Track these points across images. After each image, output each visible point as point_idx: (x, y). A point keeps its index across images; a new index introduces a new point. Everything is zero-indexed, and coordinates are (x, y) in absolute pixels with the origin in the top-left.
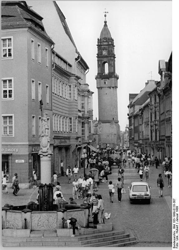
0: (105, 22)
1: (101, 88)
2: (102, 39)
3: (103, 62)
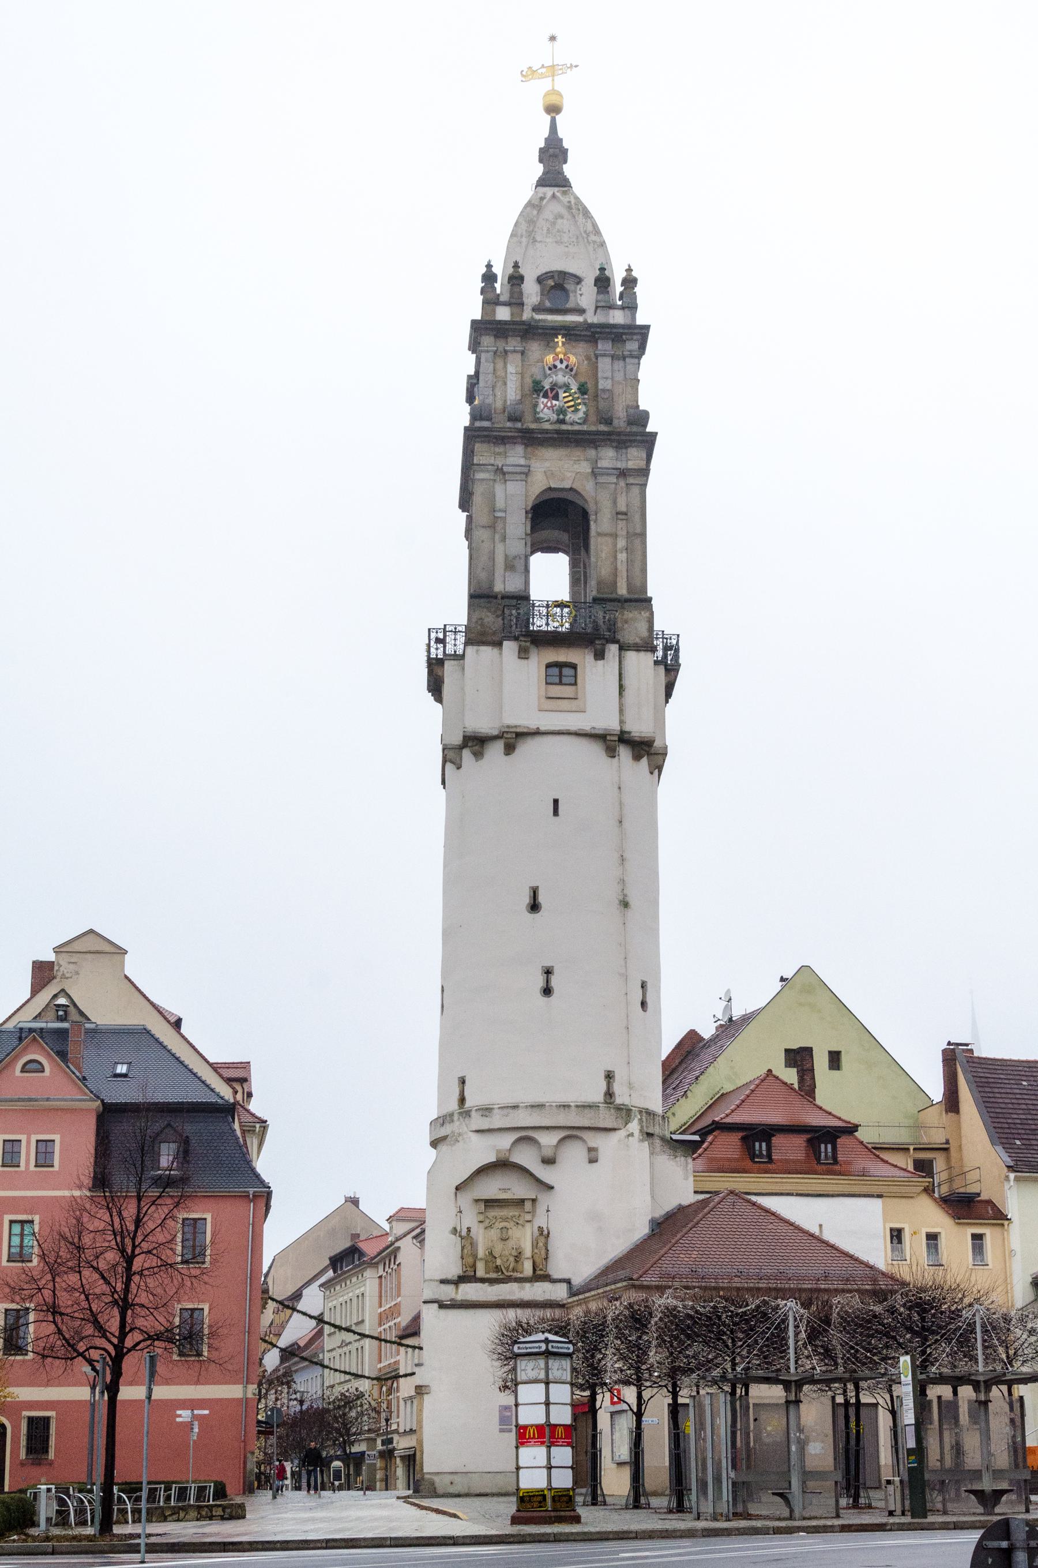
1: (512, 739)
2: (530, 275)
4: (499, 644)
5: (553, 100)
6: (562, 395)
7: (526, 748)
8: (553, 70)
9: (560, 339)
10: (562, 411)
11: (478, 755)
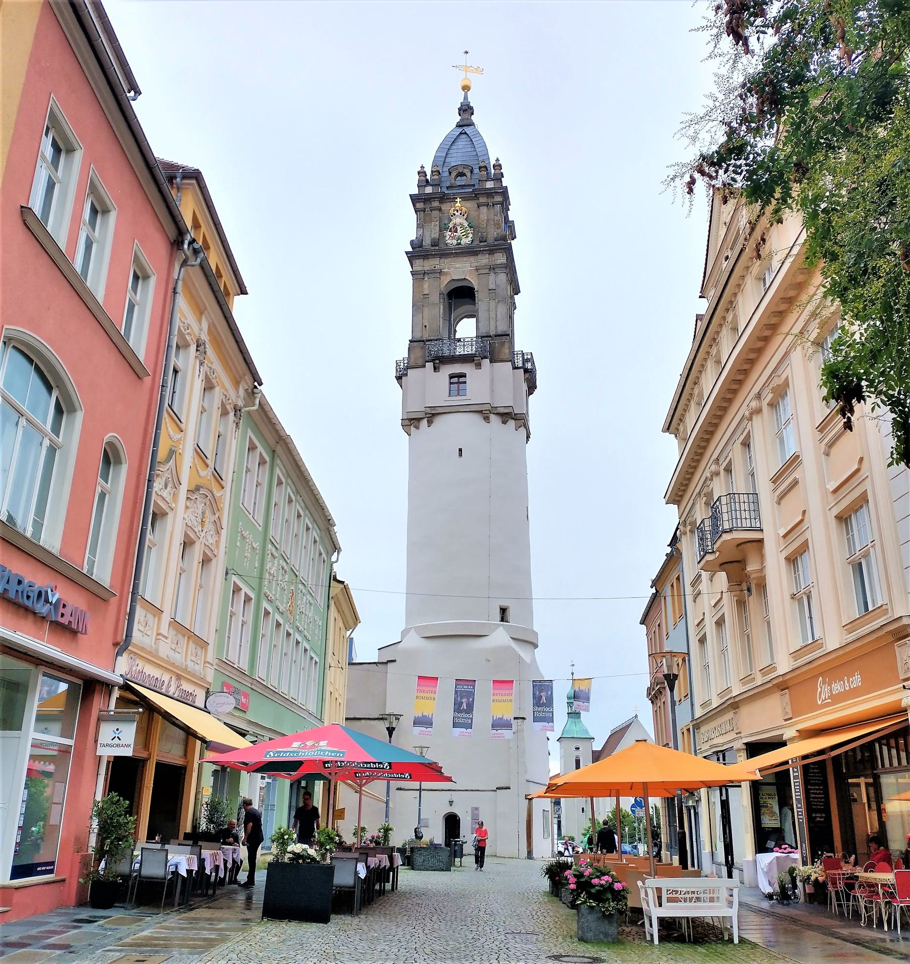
0: (466, 110)
1: (431, 416)
3: (445, 280)
4: (424, 366)
5: (466, 83)
6: (459, 229)
7: (439, 421)
8: (466, 68)
9: (458, 200)
10: (459, 238)
11: (417, 427)
